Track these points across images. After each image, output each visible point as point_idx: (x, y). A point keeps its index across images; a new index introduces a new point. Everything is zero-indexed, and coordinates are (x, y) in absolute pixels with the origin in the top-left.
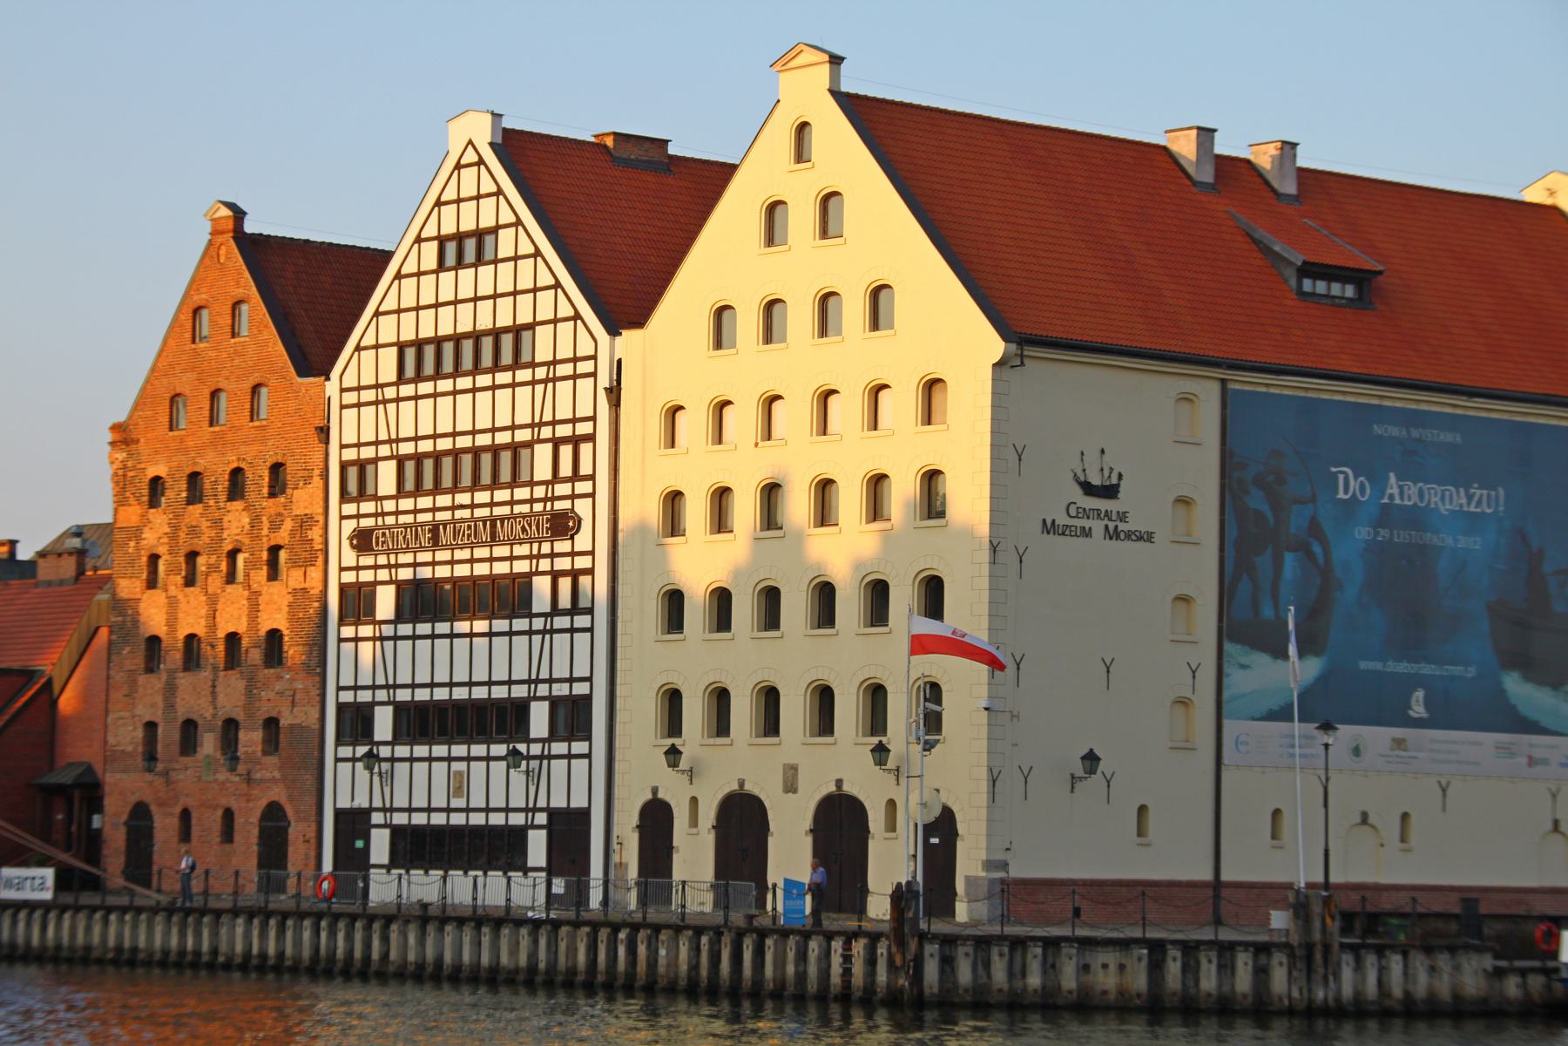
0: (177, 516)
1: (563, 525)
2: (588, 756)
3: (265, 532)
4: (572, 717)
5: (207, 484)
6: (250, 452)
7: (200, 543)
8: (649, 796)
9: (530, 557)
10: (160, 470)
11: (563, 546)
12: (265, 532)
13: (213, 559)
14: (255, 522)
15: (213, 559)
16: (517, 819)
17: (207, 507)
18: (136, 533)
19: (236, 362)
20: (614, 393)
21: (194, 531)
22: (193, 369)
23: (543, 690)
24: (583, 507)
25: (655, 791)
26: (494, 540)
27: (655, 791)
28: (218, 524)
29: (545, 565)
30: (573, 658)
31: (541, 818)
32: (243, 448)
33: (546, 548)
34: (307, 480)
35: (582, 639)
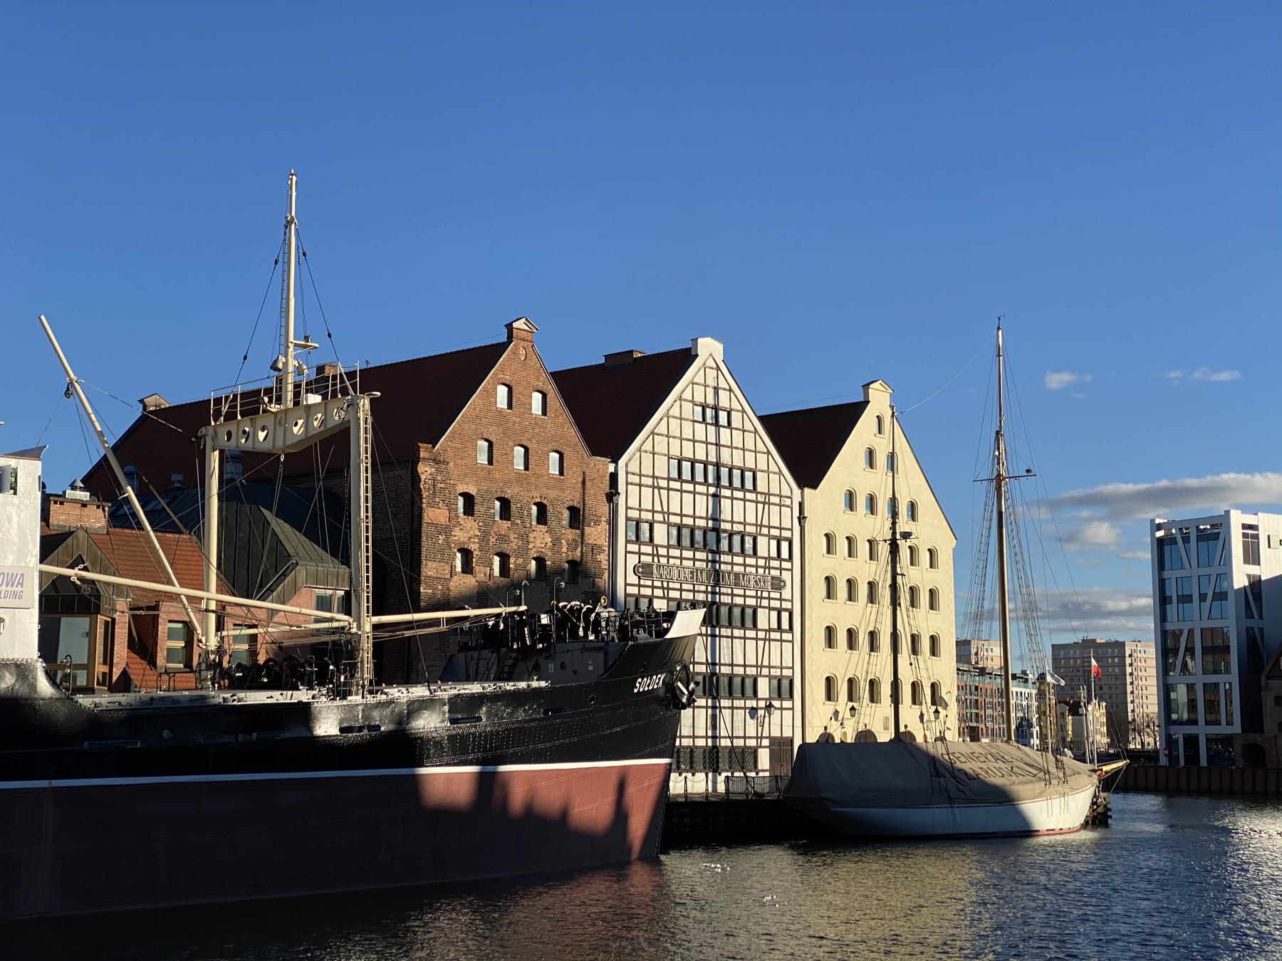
0: (485, 525)
1: (778, 584)
2: (792, 709)
3: (564, 550)
4: (783, 689)
5: (513, 507)
6: (553, 494)
7: (506, 548)
8: (822, 731)
9: (757, 597)
10: (472, 490)
11: (775, 595)
12: (564, 550)
13: (520, 561)
14: (556, 541)
15: (520, 561)
16: (752, 743)
17: (514, 524)
18: (447, 531)
19: (537, 430)
20: (802, 518)
21: (503, 538)
22: (499, 425)
23: (765, 671)
24: (786, 576)
25: (826, 728)
26: (737, 584)
27: (826, 728)
28: (524, 538)
29: (765, 603)
30: (781, 656)
31: (766, 742)
32: (545, 491)
33: (765, 594)
34: (597, 522)
35: (787, 646)
